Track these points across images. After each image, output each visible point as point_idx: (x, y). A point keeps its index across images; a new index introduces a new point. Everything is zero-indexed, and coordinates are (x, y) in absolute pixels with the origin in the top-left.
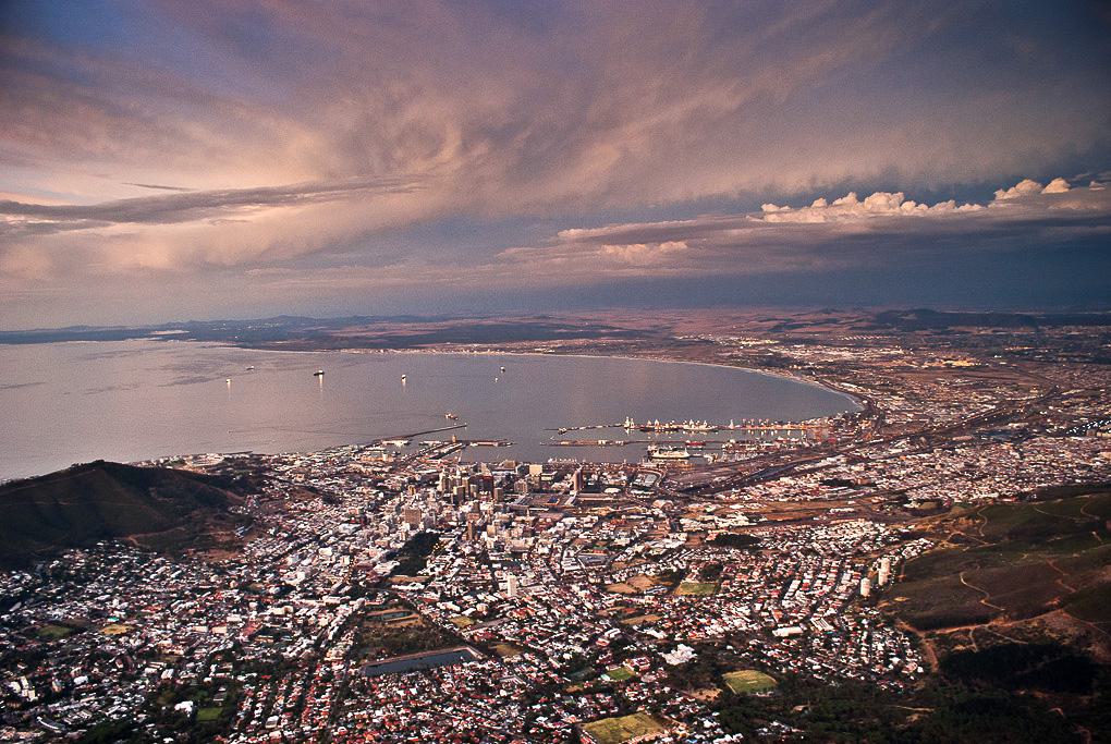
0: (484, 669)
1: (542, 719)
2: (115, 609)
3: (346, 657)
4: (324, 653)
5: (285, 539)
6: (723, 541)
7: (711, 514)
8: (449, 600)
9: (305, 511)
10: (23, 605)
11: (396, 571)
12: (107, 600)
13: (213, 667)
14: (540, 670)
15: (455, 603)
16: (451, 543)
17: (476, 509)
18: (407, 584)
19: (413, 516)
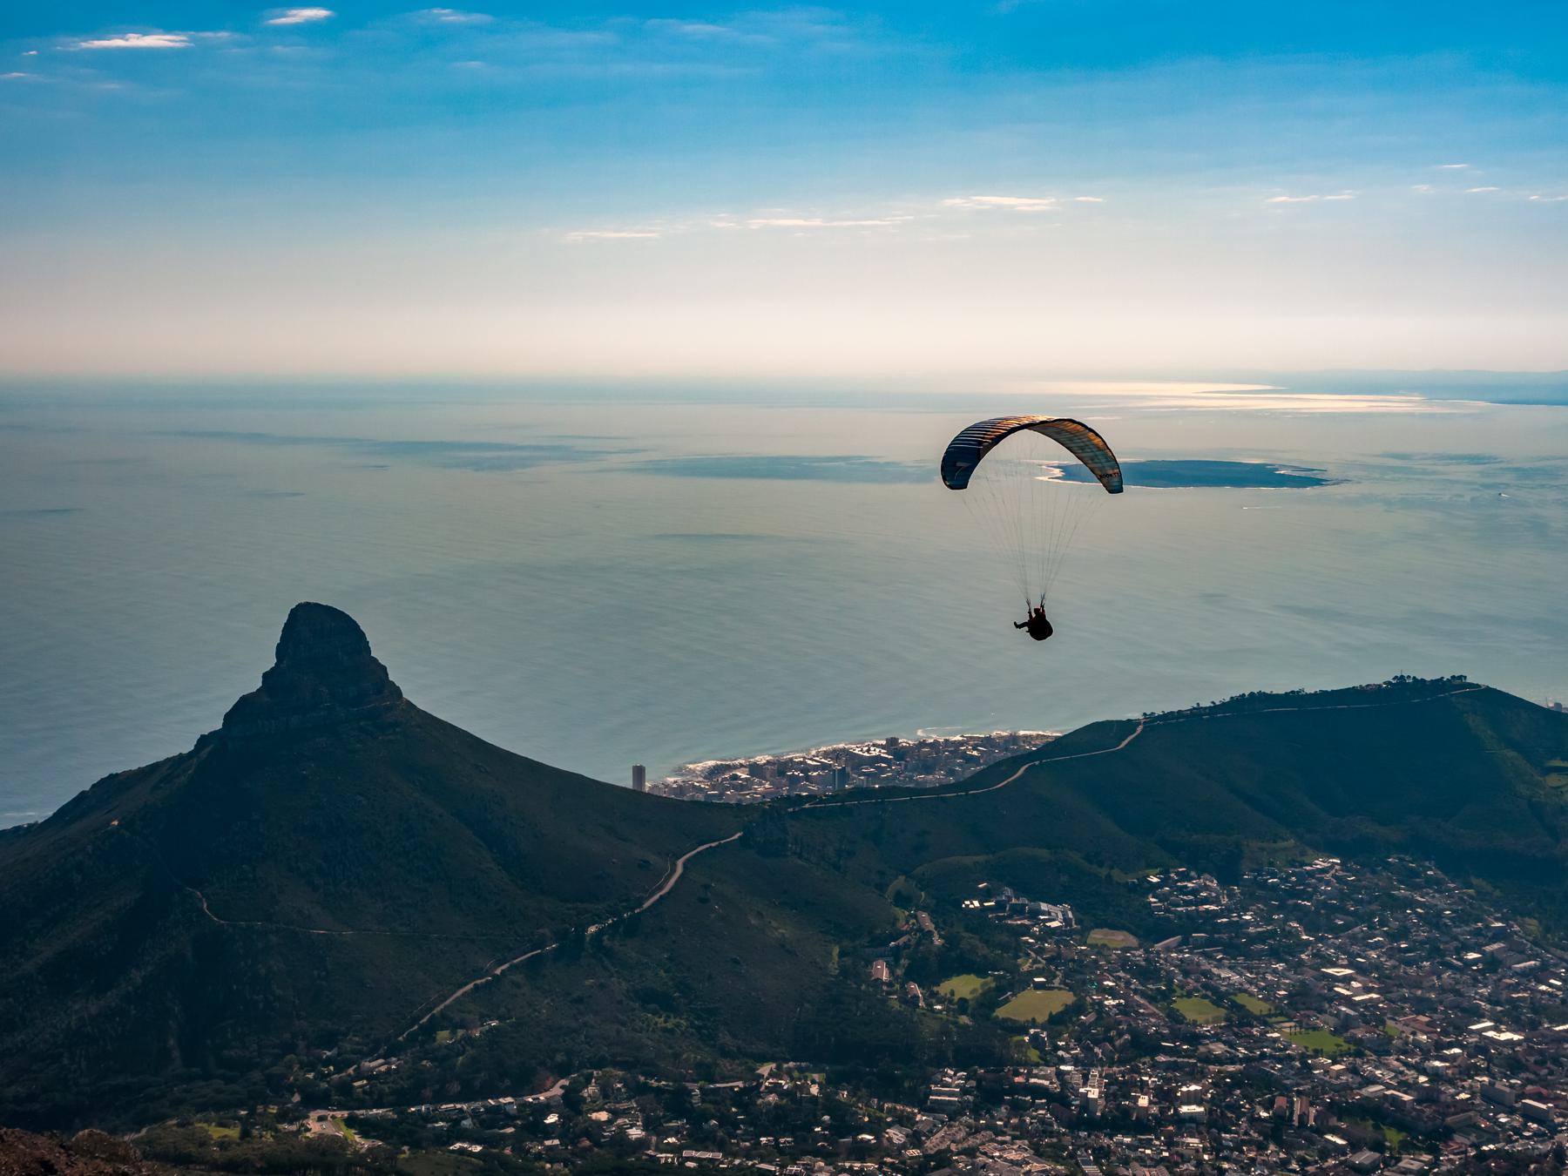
2: (1347, 1001)
10: (1185, 942)
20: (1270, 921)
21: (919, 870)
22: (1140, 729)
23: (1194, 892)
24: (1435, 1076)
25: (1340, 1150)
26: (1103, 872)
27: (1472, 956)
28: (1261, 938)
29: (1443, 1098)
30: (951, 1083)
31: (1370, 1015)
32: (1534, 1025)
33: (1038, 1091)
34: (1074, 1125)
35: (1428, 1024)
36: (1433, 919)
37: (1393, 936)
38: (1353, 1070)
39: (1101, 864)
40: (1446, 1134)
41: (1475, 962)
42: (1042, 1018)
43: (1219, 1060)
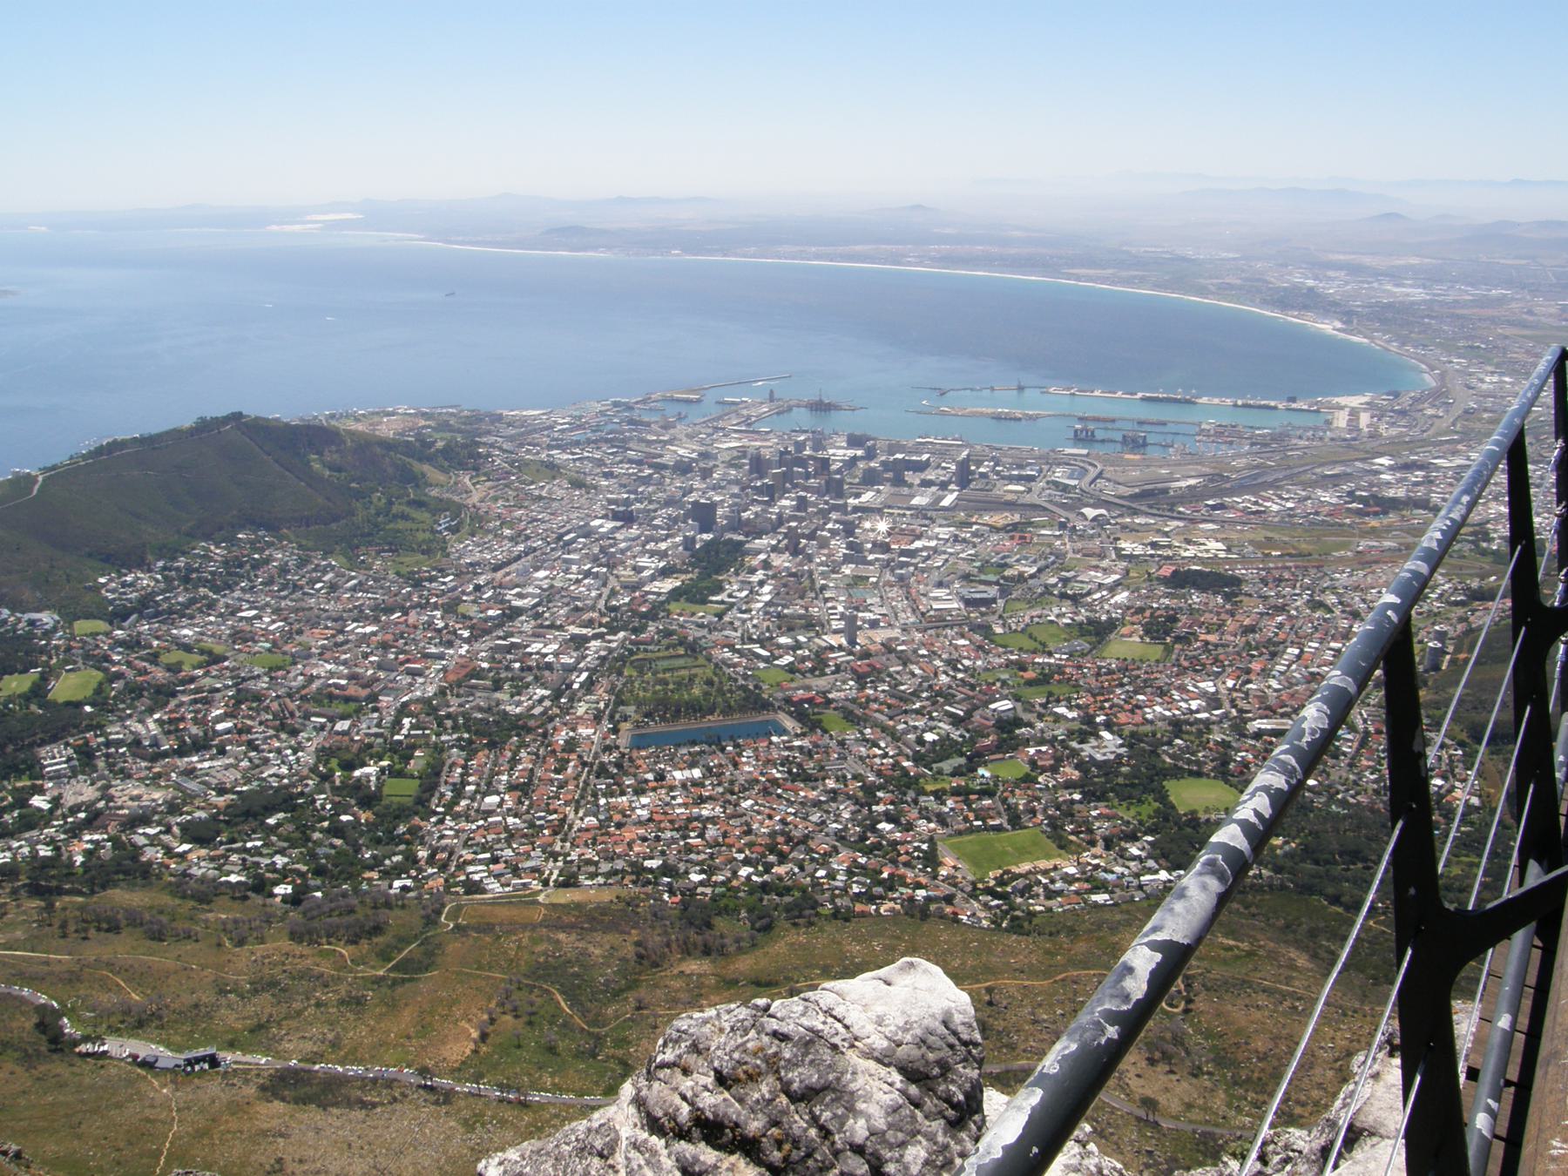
0: (801, 748)
1: (884, 826)
3: (598, 718)
4: (566, 710)
5: (511, 539)
6: (1182, 580)
7: (1166, 534)
8: (752, 641)
9: (540, 498)
11: (675, 594)
12: (255, 617)
13: (406, 721)
14: (885, 755)
15: (763, 647)
16: (762, 557)
17: (802, 504)
18: (693, 614)
19: (704, 515)
24: (345, 663)
25: (322, 727)
30: (55, 758)
31: (288, 636)
32: (376, 620)
33: (119, 743)
34: (155, 758)
40: (373, 698)
43: (218, 690)
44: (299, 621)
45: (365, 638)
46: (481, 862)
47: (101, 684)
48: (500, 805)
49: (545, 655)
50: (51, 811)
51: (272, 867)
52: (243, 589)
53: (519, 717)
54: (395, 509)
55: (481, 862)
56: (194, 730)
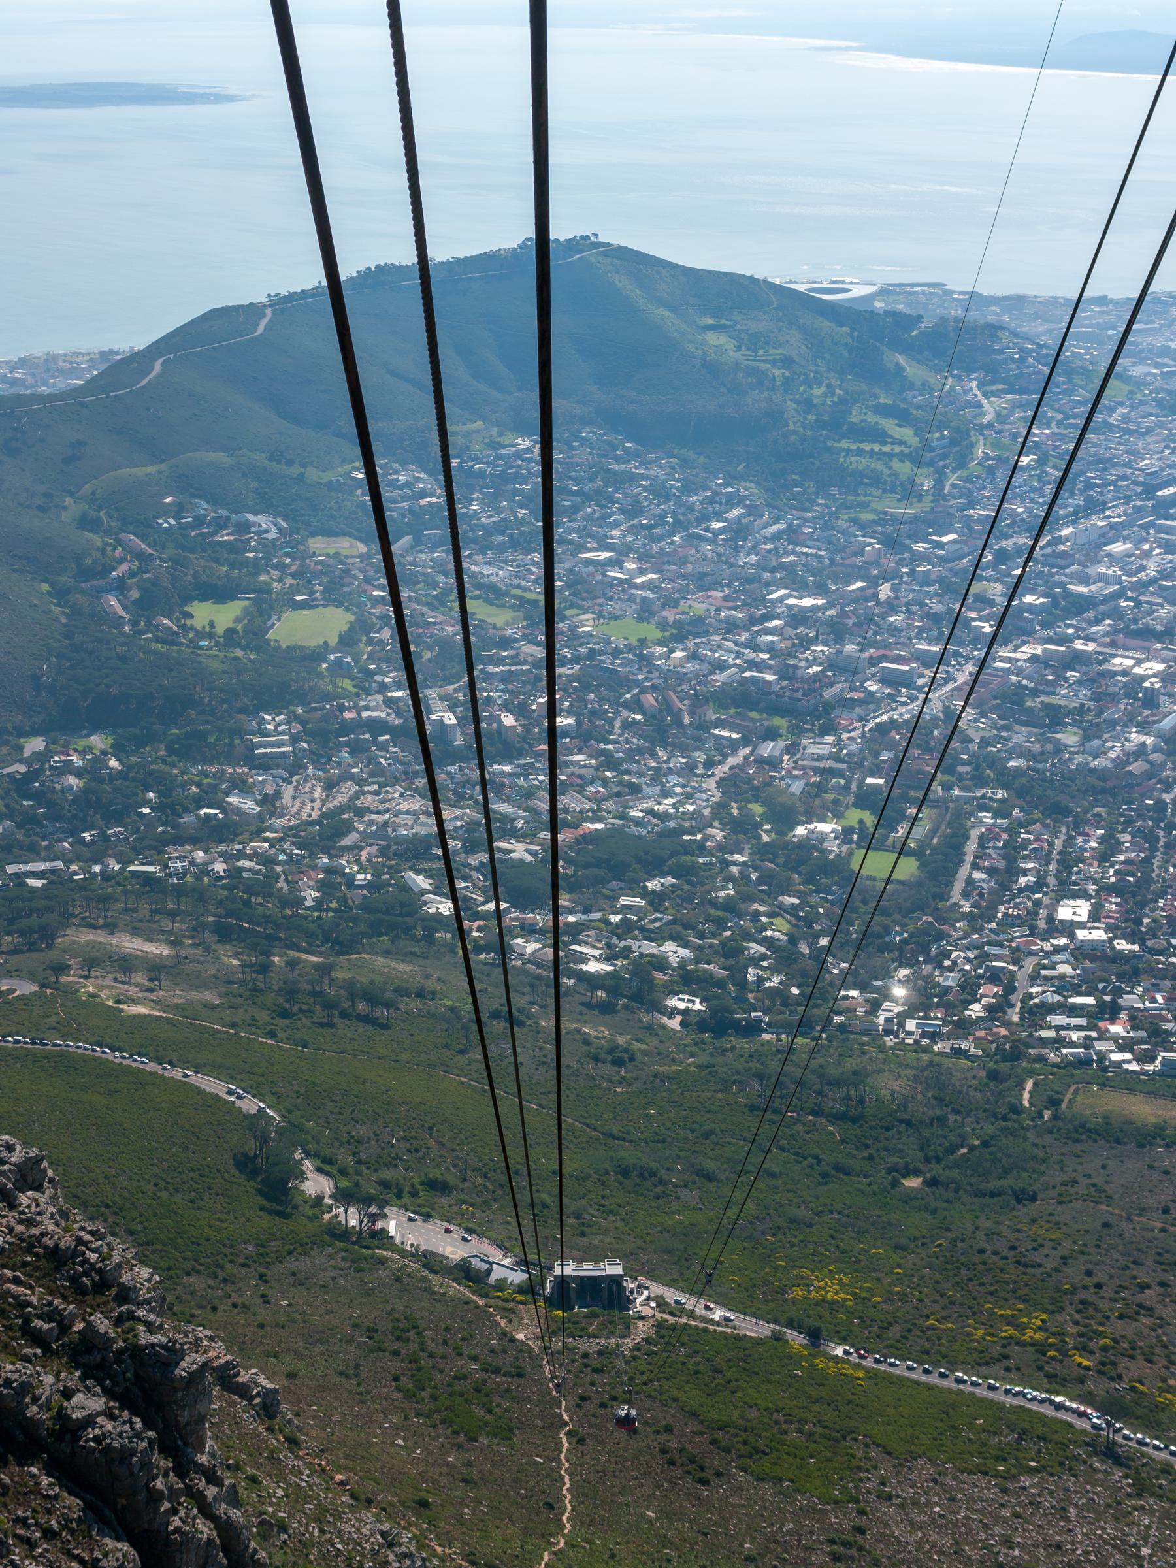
12: (609, 563)
20: (499, 511)
21: (88, 488)
22: (269, 311)
23: (406, 485)
26: (295, 470)
27: (718, 525)
28: (499, 528)
29: (799, 673)
32: (820, 590)
33: (377, 727)
35: (725, 598)
36: (660, 492)
37: (633, 511)
38: (694, 656)
39: (290, 463)
41: (722, 531)
42: (333, 641)
44: (685, 577)
45: (798, 618)
46: (1074, 1011)
47: (352, 628)
48: (1095, 916)
49: (1144, 678)
50: (260, 818)
51: (660, 963)
52: (589, 518)
53: (1101, 774)
54: (855, 417)
55: (1074, 1011)
56: (508, 720)
